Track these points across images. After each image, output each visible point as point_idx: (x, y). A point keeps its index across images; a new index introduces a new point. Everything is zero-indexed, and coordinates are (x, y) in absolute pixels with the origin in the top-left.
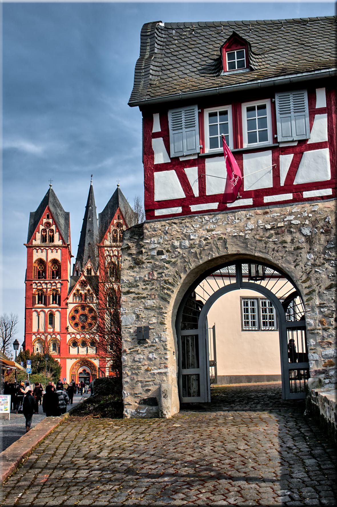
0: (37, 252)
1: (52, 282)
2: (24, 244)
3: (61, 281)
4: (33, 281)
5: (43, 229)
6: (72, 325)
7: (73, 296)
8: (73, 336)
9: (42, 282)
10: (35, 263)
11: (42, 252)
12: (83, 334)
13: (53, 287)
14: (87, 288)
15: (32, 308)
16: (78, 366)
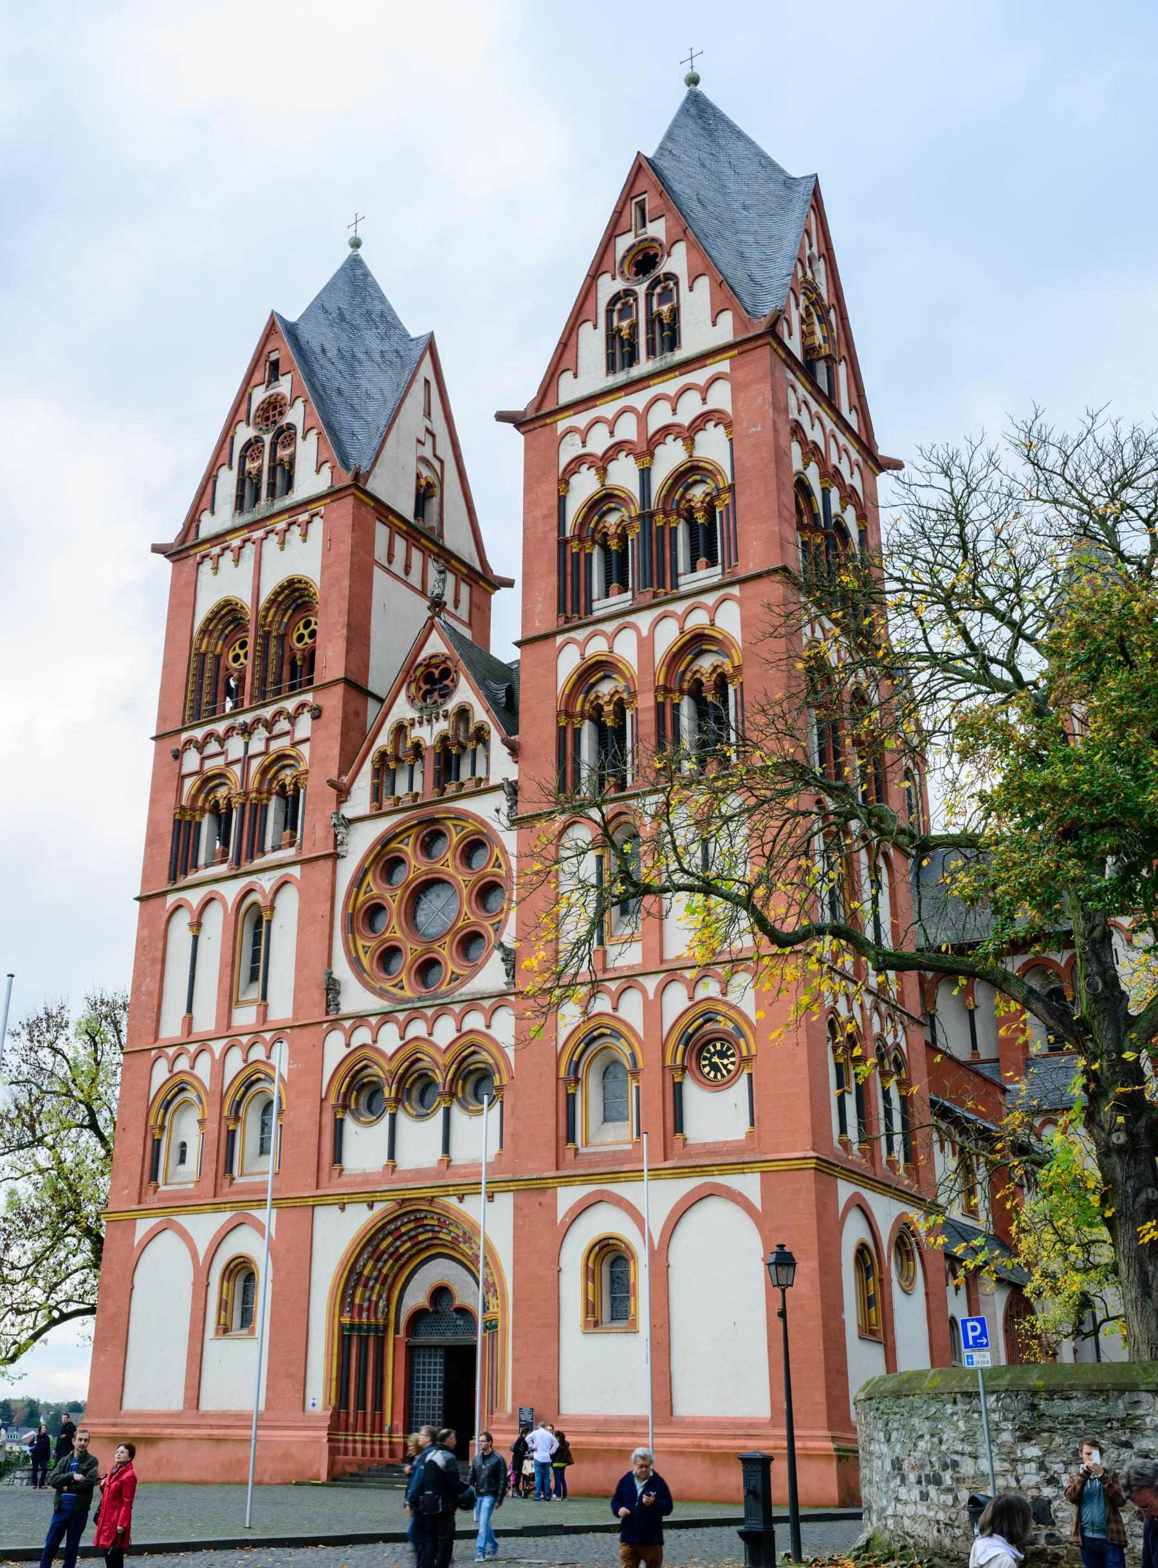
0: (216, 569)
1: (267, 713)
2: (156, 549)
3: (309, 697)
4: (185, 736)
5: (248, 445)
6: (365, 961)
7: (377, 773)
8: (362, 1036)
9: (220, 727)
10: (204, 631)
11: (237, 561)
12: (415, 1013)
13: (275, 745)
14: (451, 705)
15: (164, 894)
16: (396, 1256)
